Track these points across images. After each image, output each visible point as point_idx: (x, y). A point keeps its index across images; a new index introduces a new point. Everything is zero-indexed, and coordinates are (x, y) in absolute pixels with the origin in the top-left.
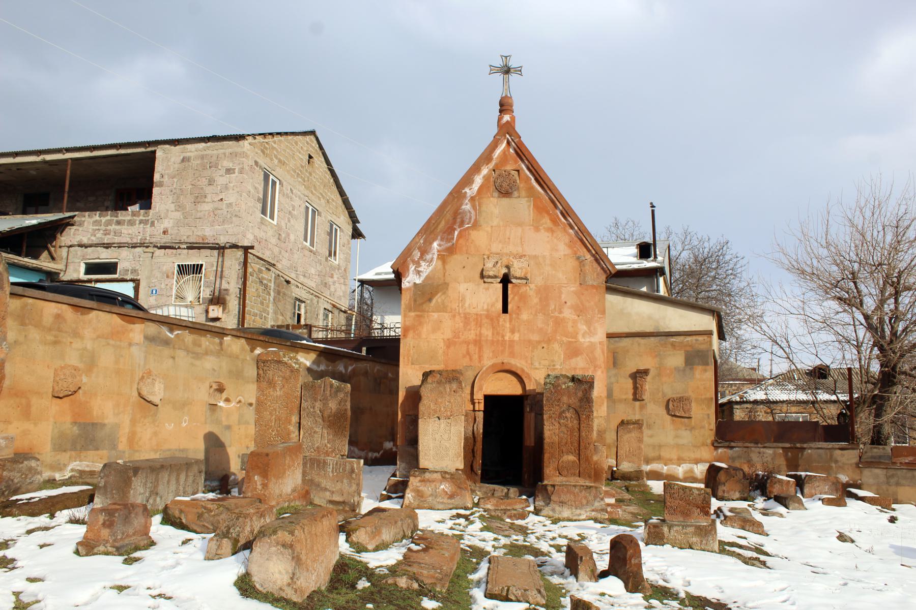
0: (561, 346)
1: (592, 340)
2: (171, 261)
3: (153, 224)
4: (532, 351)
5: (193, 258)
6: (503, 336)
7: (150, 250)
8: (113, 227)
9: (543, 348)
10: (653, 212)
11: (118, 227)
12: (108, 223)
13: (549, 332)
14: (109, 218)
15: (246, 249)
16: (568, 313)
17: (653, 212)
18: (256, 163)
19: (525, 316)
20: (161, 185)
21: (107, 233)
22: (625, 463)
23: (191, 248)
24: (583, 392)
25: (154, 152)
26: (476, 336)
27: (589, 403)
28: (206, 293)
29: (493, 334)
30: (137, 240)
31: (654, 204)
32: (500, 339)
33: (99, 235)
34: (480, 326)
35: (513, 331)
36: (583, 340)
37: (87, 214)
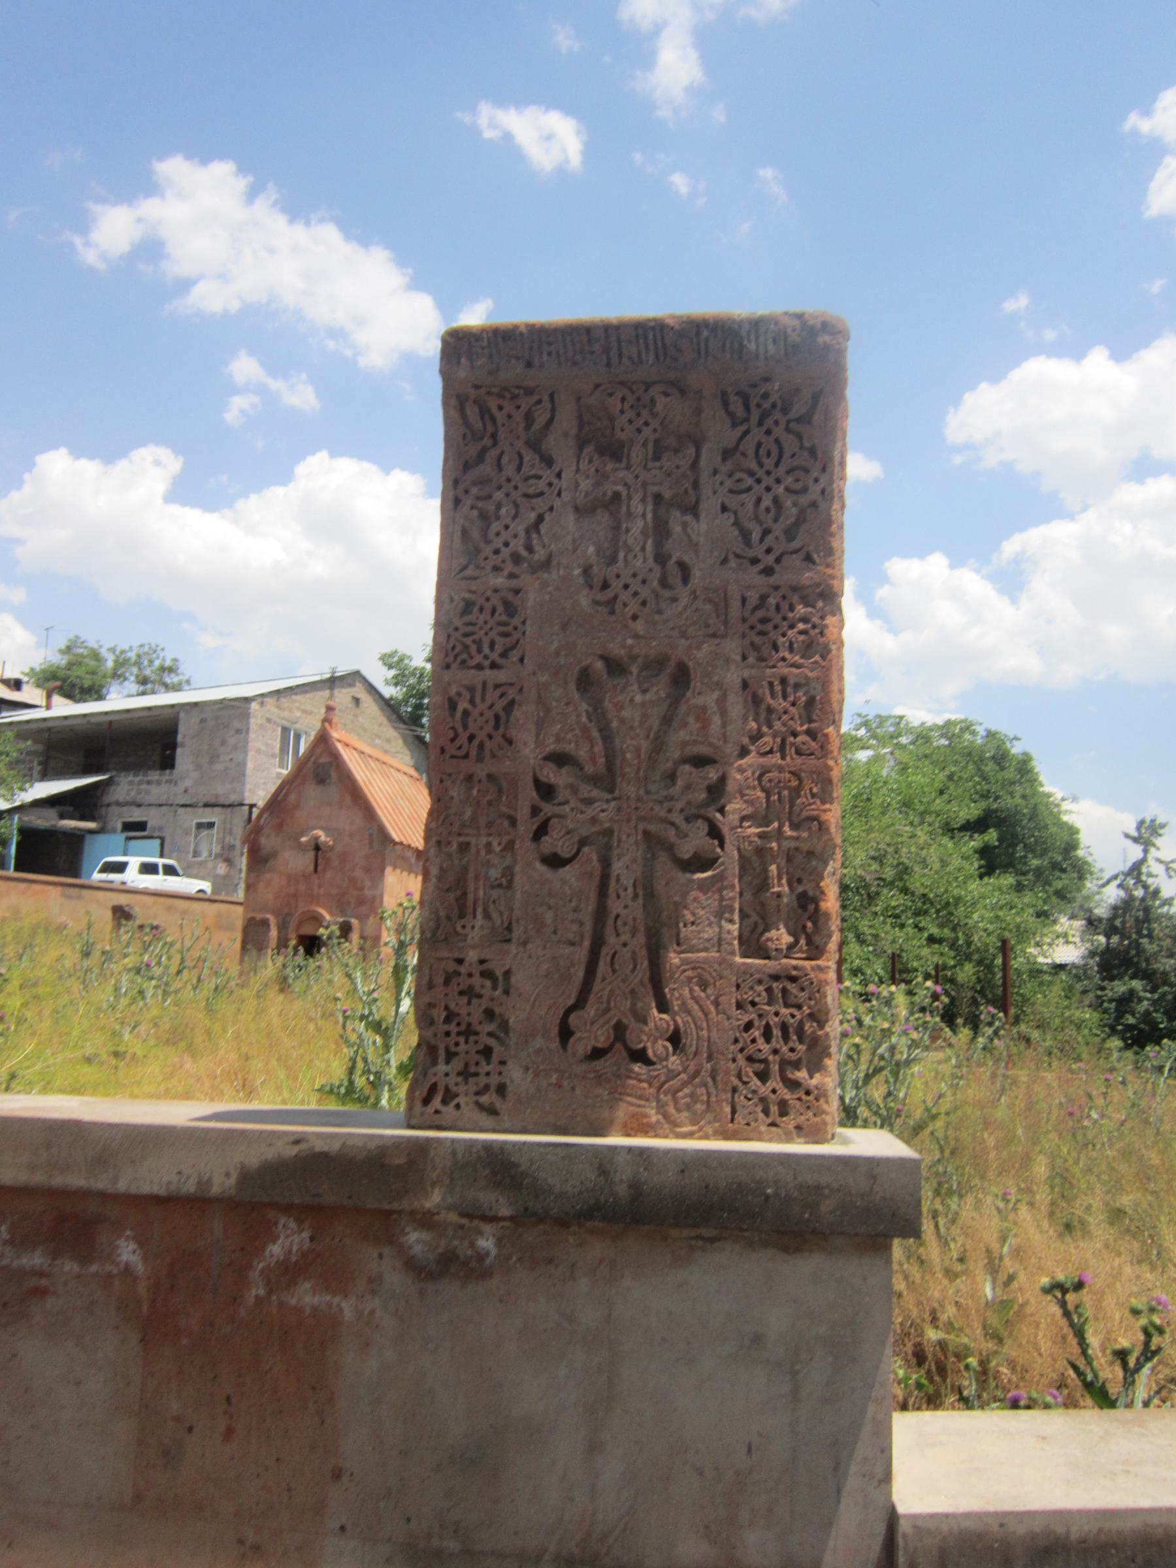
2: (191, 819)
3: (176, 783)
5: (208, 816)
7: (173, 809)
8: (144, 787)
11: (149, 787)
12: (140, 783)
14: (140, 778)
15: (252, 806)
16: (358, 873)
18: (269, 720)
19: (328, 875)
20: (183, 745)
21: (139, 792)
23: (206, 805)
25: (178, 713)
28: (216, 849)
30: (163, 800)
33: (133, 793)
35: (319, 887)
37: (123, 774)
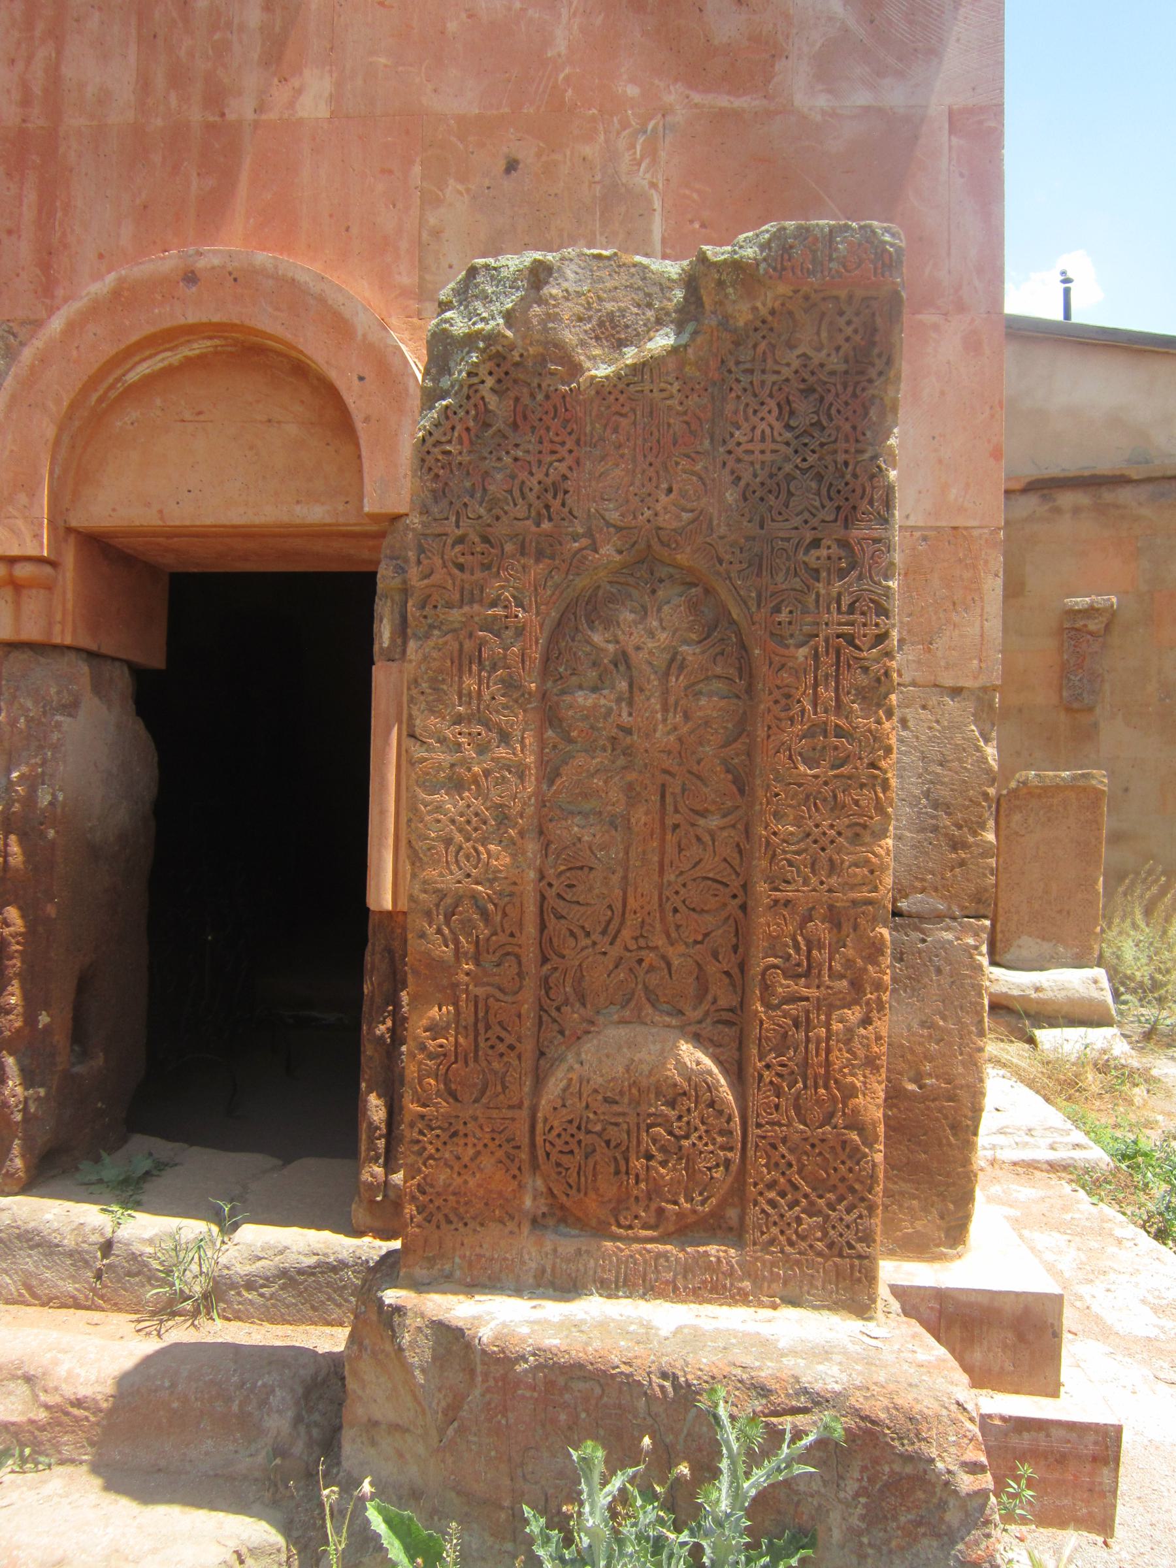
0: (651, 151)
1: (895, 96)
4: (432, 200)
6: (215, 98)
9: (512, 166)
10: (1067, 292)
13: (560, 46)
17: (1067, 292)
24: (786, 409)
26: (26, 102)
27: (848, 516)
29: (144, 85)
31: (1070, 275)
32: (196, 115)
34: (56, 35)
36: (822, 101)
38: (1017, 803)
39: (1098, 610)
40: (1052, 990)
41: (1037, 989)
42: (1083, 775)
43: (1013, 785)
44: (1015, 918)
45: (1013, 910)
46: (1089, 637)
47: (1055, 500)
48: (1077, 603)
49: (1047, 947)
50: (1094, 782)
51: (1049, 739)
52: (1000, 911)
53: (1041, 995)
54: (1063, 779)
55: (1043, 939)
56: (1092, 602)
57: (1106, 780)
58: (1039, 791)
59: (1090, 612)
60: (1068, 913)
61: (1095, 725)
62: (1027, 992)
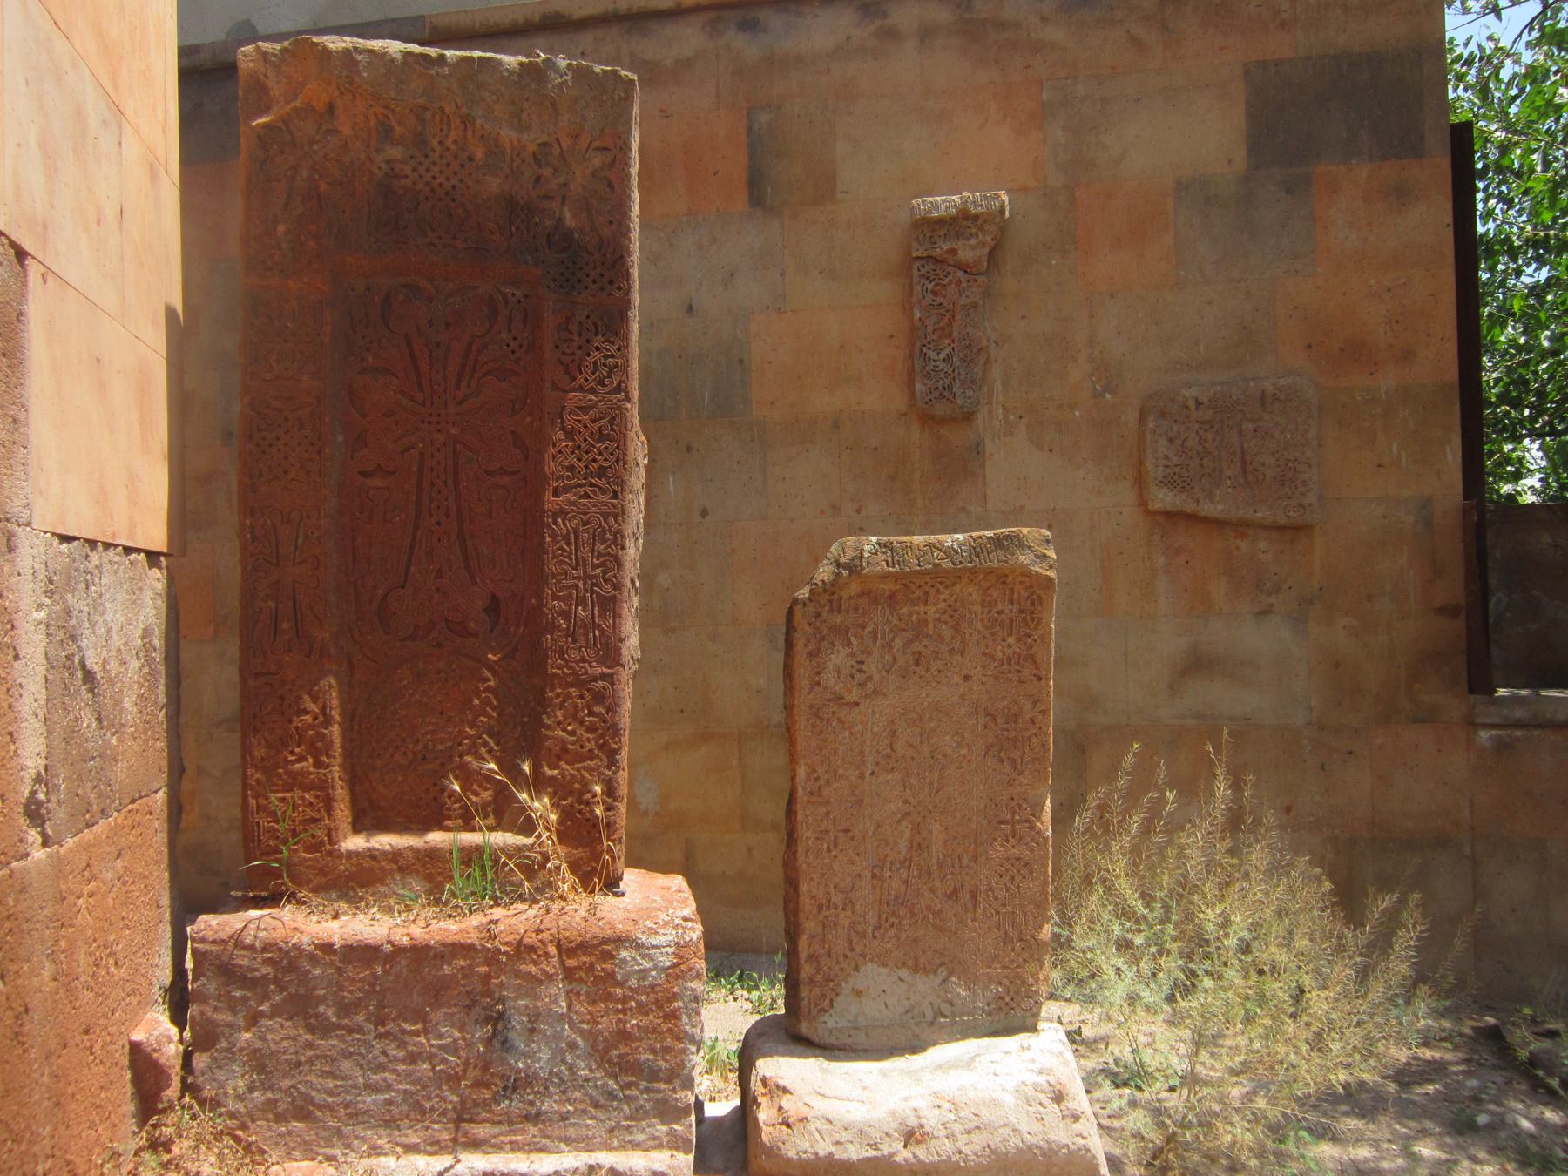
22: (873, 976)
38: (837, 619)
39: (976, 217)
40: (951, 1136)
41: (911, 1136)
42: (998, 541)
43: (824, 572)
44: (844, 919)
45: (837, 899)
46: (960, 274)
47: (885, 16)
48: (935, 205)
49: (925, 987)
50: (1025, 558)
51: (892, 478)
52: (806, 902)
53: (921, 1152)
54: (950, 553)
55: (916, 969)
56: (965, 202)
57: (1052, 553)
58: (889, 586)
59: (962, 222)
60: (974, 896)
61: (978, 448)
62: (885, 1149)
